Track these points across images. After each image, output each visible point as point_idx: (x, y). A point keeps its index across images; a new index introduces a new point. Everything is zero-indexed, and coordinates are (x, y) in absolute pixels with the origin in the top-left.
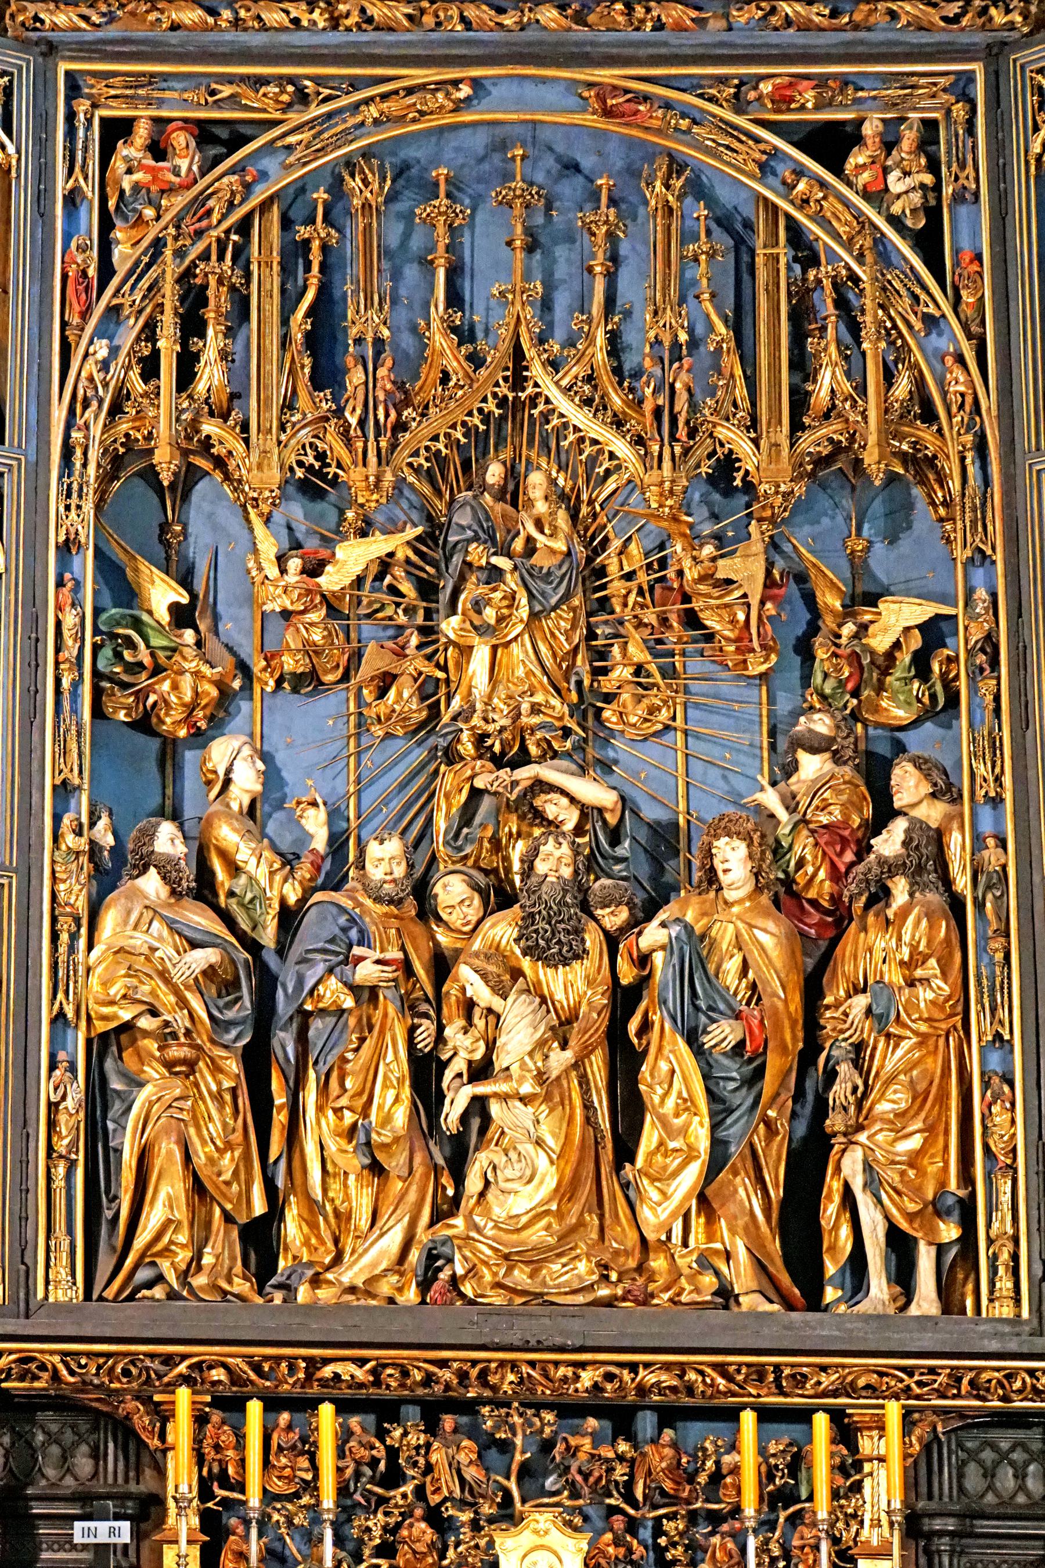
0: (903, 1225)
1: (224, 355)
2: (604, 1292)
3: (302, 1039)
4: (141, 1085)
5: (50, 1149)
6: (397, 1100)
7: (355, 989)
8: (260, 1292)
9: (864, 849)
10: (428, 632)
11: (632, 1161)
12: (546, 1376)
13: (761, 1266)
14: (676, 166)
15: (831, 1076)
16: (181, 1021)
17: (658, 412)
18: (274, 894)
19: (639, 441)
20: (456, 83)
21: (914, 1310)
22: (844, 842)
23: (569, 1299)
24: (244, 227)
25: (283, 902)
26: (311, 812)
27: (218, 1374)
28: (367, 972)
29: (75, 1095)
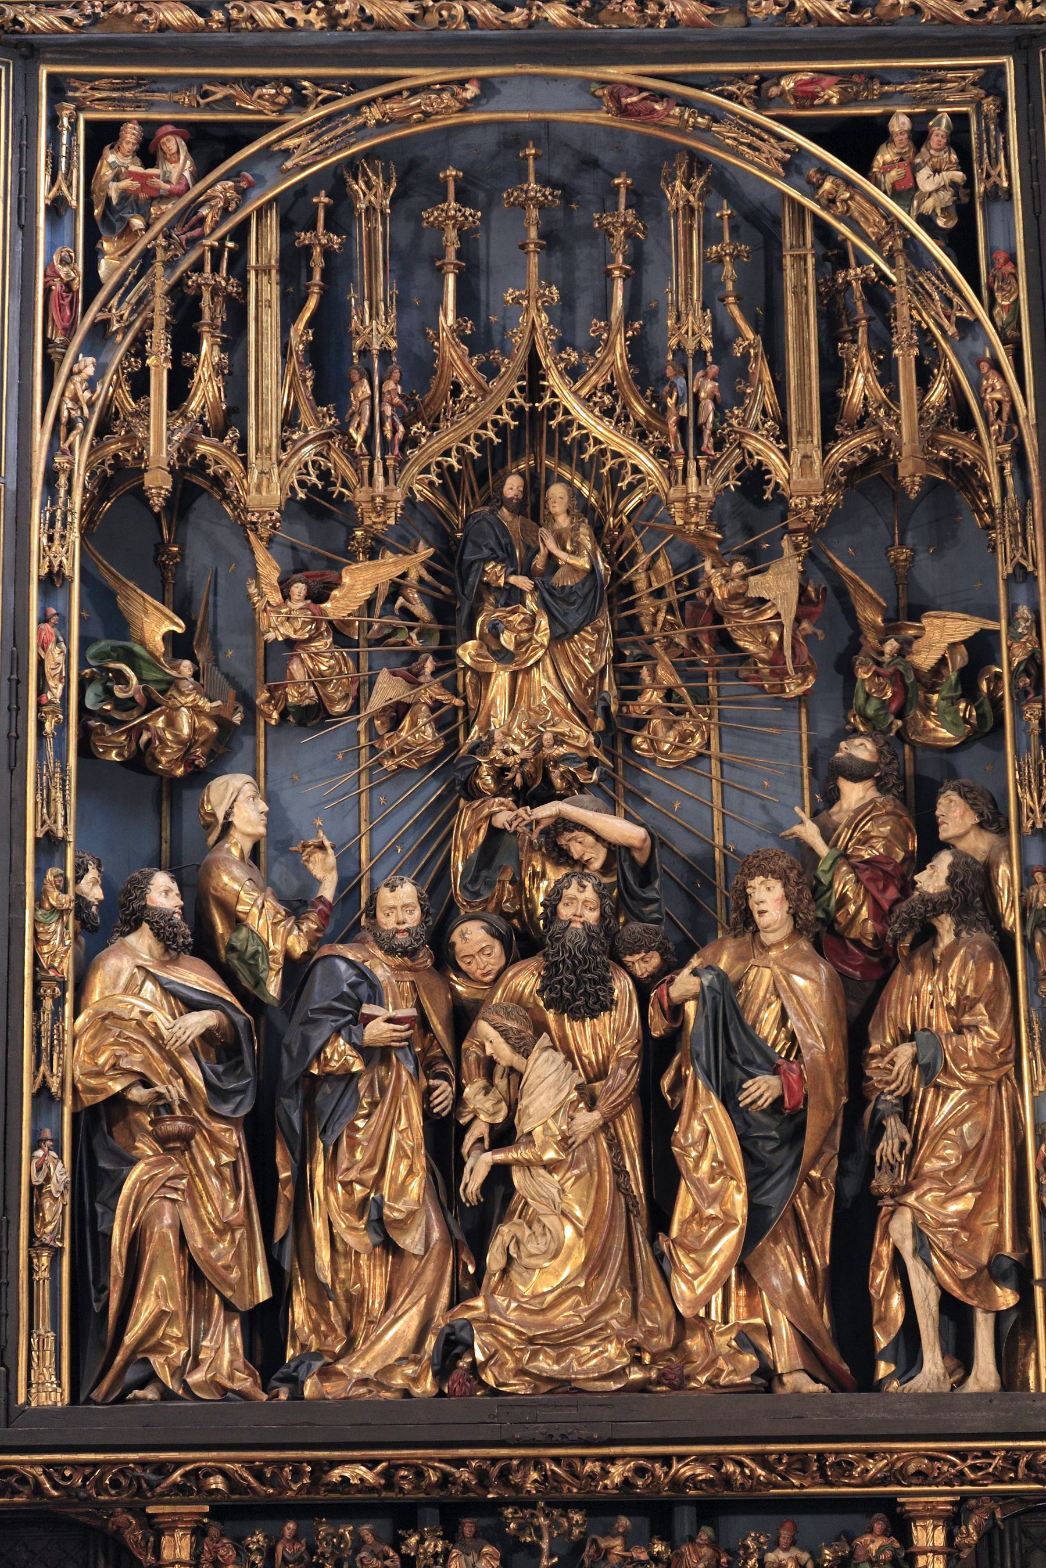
0: (957, 1292)
1: (218, 370)
2: (636, 1375)
3: (309, 1106)
4: (132, 1163)
5: (32, 1235)
6: (410, 1172)
7: (366, 1052)
8: (265, 1390)
9: (907, 887)
10: (446, 658)
11: (667, 1231)
12: (574, 1474)
13: (805, 1343)
14: (698, 163)
15: (878, 1130)
16: (176, 1091)
17: (682, 423)
18: (275, 946)
19: (662, 453)
20: (462, 83)
21: (971, 1386)
22: (888, 877)
23: (599, 1385)
24: (241, 233)
25: (288, 955)
26: (319, 856)
27: (217, 1483)
28: (377, 1031)
29: (60, 1172)
